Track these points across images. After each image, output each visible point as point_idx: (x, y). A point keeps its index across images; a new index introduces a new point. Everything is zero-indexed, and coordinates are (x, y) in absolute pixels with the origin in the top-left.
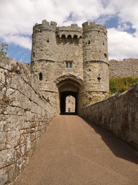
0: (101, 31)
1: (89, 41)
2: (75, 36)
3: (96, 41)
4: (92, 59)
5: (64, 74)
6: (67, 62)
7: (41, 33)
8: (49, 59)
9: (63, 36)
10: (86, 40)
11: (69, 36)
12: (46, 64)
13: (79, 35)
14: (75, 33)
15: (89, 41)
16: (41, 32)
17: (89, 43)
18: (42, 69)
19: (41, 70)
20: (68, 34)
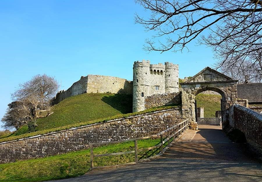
0: (176, 68)
1: (169, 75)
2: (162, 71)
3: (173, 75)
4: (171, 86)
5: (154, 93)
6: (156, 86)
7: (142, 68)
8: (147, 84)
9: (155, 71)
10: (167, 74)
11: (158, 71)
12: (146, 87)
13: (163, 70)
14: (162, 69)
15: (169, 75)
16: (142, 67)
17: (169, 76)
18: (143, 90)
19: (143, 91)
20: (157, 70)
